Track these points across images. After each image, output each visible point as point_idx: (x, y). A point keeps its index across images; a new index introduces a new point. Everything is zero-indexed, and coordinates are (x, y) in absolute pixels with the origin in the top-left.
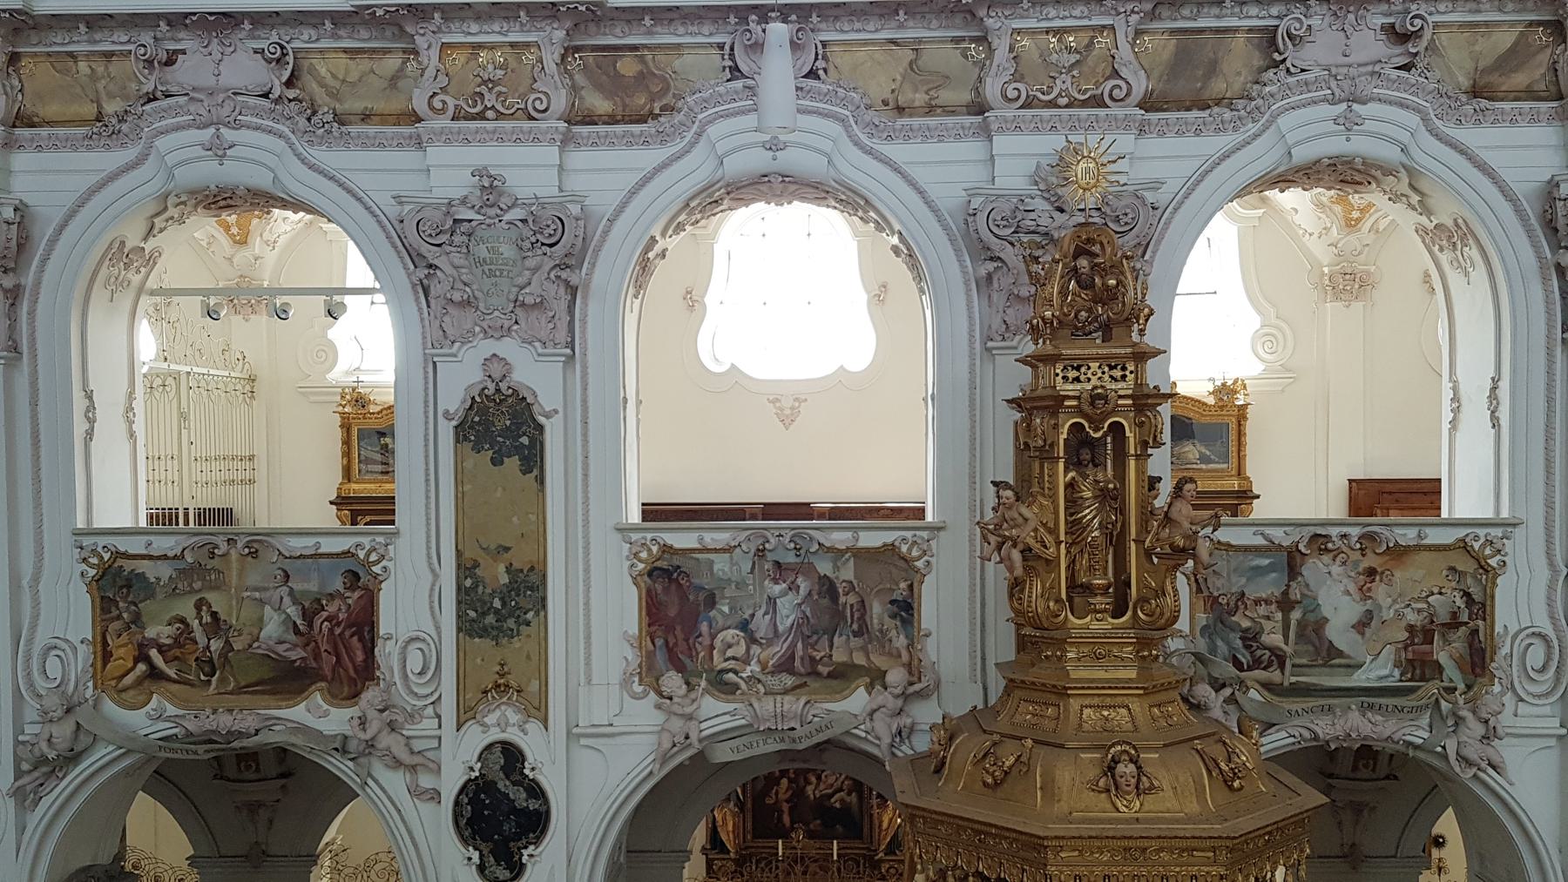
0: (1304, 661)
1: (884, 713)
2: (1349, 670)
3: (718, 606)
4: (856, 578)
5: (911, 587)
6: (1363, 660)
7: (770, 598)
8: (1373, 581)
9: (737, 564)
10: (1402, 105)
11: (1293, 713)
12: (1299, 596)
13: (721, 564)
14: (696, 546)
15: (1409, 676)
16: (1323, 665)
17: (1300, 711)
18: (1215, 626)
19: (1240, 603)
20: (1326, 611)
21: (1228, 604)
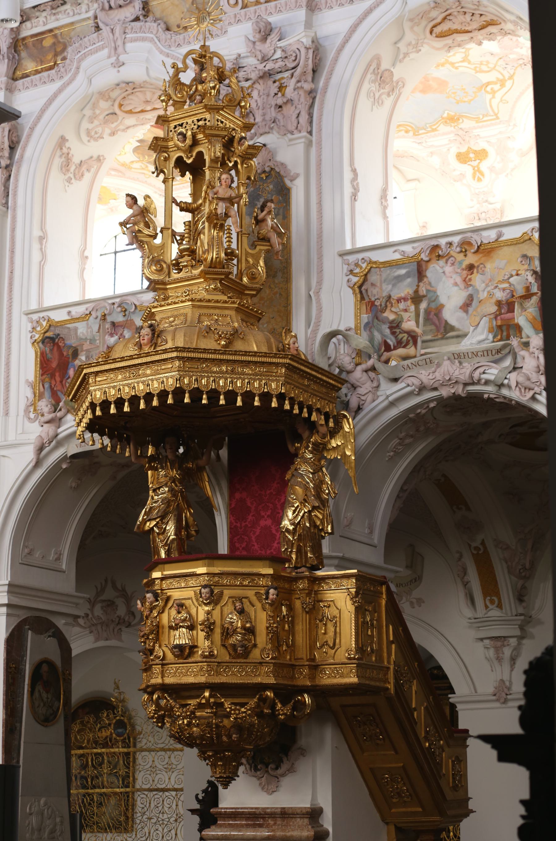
0: (429, 337)
2: (460, 339)
3: (79, 357)
6: (467, 331)
8: (472, 273)
9: (91, 327)
11: (405, 367)
12: (425, 292)
13: (82, 329)
14: (67, 317)
15: (499, 337)
16: (442, 338)
17: (410, 365)
18: (373, 321)
19: (388, 303)
20: (443, 299)
21: (381, 305)
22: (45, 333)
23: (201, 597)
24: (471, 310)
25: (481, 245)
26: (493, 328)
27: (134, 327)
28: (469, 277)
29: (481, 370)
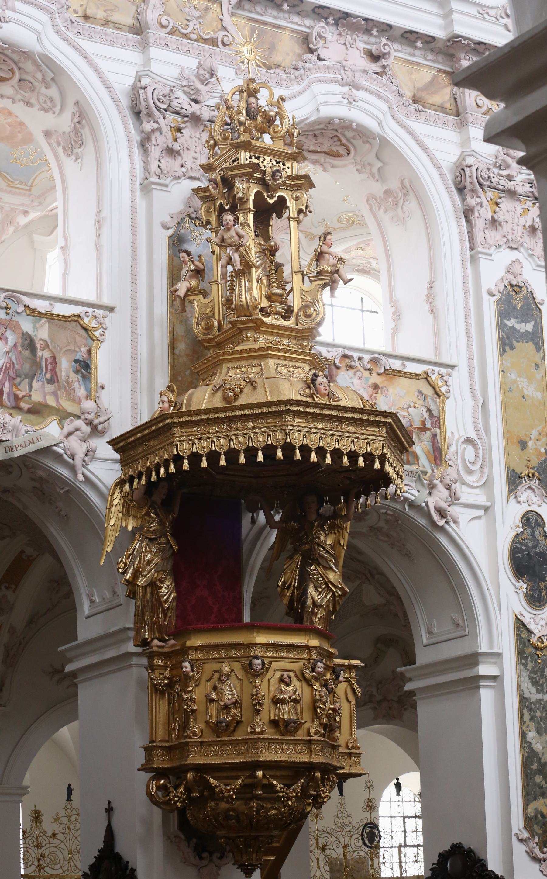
1: (77, 436)
4: (50, 338)
5: (89, 351)
8: (377, 393)
10: (379, 97)
28: (374, 395)
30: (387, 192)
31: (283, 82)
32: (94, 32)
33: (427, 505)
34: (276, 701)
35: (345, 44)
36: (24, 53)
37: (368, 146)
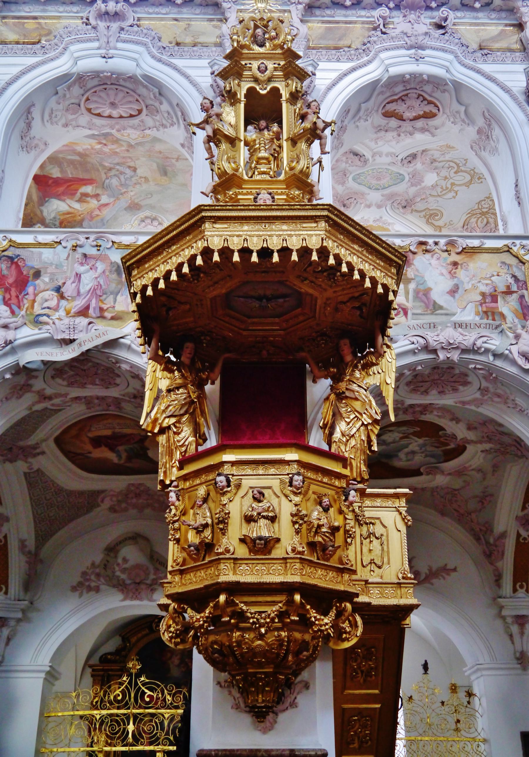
0: (419, 311)
3: (41, 278)
6: (454, 311)
7: (77, 274)
8: (456, 268)
16: (432, 314)
17: (415, 326)
20: (430, 284)
22: (3, 251)
23: (291, 485)
24: (457, 295)
25: (465, 248)
26: (479, 312)
27: (109, 262)
28: (454, 270)
29: (485, 339)
30: (479, 132)
31: (353, 57)
32: (184, 51)
33: (511, 352)
34: (249, 519)
35: (410, 22)
36: (130, 77)
37: (446, 94)
